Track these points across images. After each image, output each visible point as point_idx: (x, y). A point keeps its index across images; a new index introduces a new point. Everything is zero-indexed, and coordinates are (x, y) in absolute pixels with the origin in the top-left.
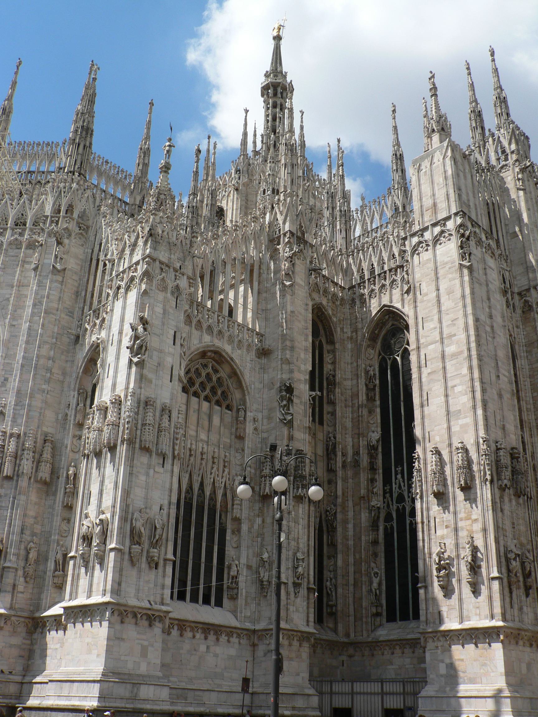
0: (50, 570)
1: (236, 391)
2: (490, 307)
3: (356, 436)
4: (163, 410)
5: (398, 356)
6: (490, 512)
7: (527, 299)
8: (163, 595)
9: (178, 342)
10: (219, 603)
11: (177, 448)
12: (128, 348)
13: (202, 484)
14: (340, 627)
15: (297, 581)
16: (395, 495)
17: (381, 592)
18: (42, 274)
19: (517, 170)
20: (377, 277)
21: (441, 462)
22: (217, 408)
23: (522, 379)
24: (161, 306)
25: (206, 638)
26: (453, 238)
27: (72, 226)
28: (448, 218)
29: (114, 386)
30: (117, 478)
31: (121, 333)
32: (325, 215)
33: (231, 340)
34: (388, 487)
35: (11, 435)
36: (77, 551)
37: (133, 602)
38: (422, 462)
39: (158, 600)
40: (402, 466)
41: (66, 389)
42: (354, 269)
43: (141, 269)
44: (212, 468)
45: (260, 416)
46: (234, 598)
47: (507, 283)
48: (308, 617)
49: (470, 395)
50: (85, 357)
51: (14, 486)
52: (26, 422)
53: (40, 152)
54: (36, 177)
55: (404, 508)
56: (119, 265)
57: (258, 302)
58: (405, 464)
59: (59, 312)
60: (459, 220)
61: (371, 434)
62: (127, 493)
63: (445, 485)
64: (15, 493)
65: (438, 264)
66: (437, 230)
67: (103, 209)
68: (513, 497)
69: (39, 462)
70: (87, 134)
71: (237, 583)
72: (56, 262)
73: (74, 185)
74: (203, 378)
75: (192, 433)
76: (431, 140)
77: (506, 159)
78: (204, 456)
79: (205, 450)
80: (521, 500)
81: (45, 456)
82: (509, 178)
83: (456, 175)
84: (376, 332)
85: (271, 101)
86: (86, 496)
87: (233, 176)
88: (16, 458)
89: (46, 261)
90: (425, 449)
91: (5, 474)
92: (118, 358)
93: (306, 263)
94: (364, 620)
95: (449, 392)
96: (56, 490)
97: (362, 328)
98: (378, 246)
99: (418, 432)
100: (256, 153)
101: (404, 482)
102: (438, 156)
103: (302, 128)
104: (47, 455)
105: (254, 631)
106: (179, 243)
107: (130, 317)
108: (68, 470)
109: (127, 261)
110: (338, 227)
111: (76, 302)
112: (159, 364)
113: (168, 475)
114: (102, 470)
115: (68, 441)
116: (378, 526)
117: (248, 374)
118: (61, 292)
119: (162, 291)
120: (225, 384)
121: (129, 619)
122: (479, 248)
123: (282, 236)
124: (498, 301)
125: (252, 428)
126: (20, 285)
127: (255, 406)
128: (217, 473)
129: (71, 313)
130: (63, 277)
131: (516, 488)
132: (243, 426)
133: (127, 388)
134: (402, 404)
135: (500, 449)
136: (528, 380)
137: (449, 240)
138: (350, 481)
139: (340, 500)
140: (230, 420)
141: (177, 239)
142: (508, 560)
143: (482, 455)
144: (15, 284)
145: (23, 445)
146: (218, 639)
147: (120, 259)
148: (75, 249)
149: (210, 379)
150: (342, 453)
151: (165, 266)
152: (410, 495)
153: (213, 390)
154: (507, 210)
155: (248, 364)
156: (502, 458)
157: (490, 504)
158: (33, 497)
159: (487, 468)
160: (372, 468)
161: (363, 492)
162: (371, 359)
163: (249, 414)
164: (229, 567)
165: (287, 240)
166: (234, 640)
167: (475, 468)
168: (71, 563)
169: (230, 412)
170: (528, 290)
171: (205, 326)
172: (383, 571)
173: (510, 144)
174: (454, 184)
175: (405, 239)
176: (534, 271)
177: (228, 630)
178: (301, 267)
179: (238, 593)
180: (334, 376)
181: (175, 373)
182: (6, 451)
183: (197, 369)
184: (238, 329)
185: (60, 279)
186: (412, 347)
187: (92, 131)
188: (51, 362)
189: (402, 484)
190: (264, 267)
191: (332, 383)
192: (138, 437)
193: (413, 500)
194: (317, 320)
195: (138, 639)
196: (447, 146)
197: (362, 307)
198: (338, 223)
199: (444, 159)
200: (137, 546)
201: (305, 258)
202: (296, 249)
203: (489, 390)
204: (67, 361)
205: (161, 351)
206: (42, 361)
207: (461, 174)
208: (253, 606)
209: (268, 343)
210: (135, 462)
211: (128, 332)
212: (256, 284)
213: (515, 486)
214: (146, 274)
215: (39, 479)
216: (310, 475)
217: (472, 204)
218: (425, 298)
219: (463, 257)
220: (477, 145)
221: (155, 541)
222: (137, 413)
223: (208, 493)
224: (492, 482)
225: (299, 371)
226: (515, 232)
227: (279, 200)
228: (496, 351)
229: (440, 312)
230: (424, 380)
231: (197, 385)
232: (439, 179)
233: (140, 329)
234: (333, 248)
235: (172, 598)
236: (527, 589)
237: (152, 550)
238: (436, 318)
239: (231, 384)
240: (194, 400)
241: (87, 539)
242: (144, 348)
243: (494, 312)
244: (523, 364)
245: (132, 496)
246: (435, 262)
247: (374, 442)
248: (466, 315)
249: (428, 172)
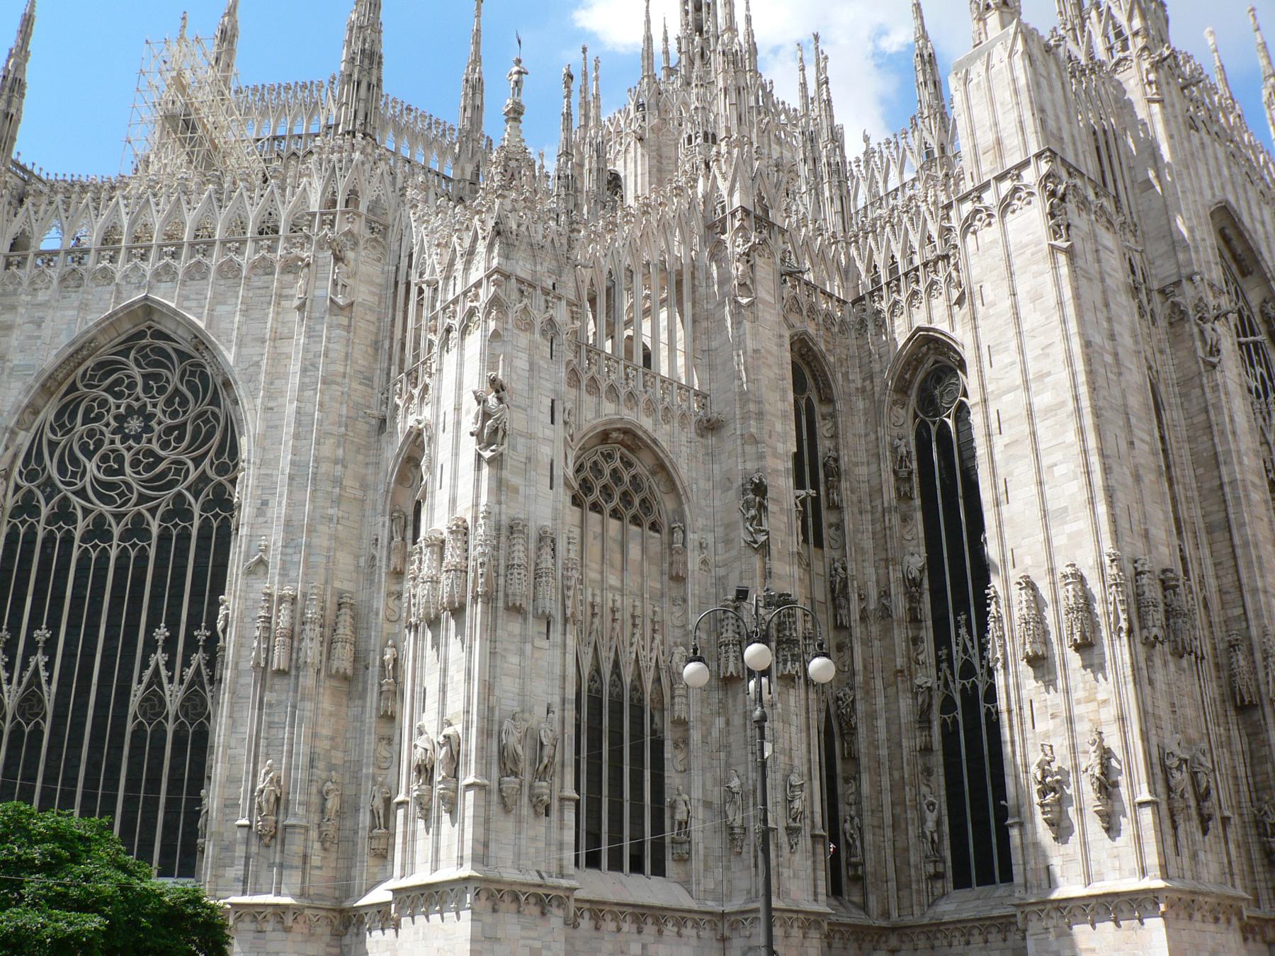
0: (364, 828)
1: (666, 498)
2: (1109, 320)
3: (883, 564)
4: (541, 539)
5: (948, 417)
6: (1131, 686)
7: (1177, 299)
8: (561, 859)
9: (559, 417)
10: (659, 870)
11: (569, 603)
12: (472, 434)
13: (616, 664)
14: (873, 901)
15: (793, 825)
16: (957, 665)
17: (941, 837)
18: (313, 315)
19: (1146, 65)
20: (902, 278)
21: (1037, 603)
22: (634, 529)
23: (1174, 445)
24: (525, 356)
25: (640, 932)
26: (1036, 200)
27: (359, 227)
28: (1025, 164)
29: (453, 502)
30: (470, 661)
31: (458, 409)
32: (801, 173)
33: (650, 408)
34: (945, 651)
35: (281, 599)
36: (408, 792)
37: (510, 874)
38: (1002, 603)
39: (554, 869)
40: (968, 612)
41: (369, 513)
42: (861, 267)
43: (485, 294)
44: (633, 634)
45: (710, 538)
46: (683, 860)
47: (1139, 273)
48: (815, 886)
49: (1083, 480)
50: (398, 455)
51: (292, 685)
52: (305, 574)
53: (292, 101)
54: (289, 145)
55: (975, 686)
56: (445, 290)
57: (694, 338)
58: (972, 609)
59: (347, 380)
60: (1044, 167)
61: (907, 558)
62: (488, 688)
63: (1046, 642)
64: (295, 697)
65: (1012, 248)
66: (1006, 186)
67: (410, 193)
68: (1169, 658)
69: (331, 642)
70: (371, 63)
71: (688, 834)
72: (335, 293)
73: (357, 156)
74: (607, 478)
75: (594, 575)
76: (985, 24)
77: (1125, 48)
78: (618, 616)
79: (618, 604)
80: (1185, 663)
81: (341, 631)
82: (1132, 82)
83: (1036, 84)
84: (907, 376)
86: (417, 696)
87: (632, 115)
88: (292, 638)
89: (318, 293)
90: (1006, 581)
91: (275, 667)
92: (456, 454)
93: (775, 263)
94: (914, 887)
95: (1045, 477)
96: (365, 689)
97: (882, 372)
98: (900, 221)
99: (992, 551)
100: (671, 71)
101: (972, 640)
102: (999, 53)
103: (749, 20)
104: (344, 630)
105: (723, 914)
106: (548, 244)
107: (474, 379)
108: (383, 654)
109: (459, 281)
110: (827, 194)
111: (376, 360)
112: (529, 459)
113: (558, 652)
114: (442, 649)
115: (380, 603)
116: (930, 722)
117: (685, 466)
118: (348, 346)
119: (526, 330)
120: (646, 485)
121: (507, 905)
122: (1084, 214)
123: (729, 217)
124: (1124, 307)
125: (698, 560)
126: (277, 338)
127: (701, 522)
128: (641, 643)
129: (368, 381)
130: (350, 319)
131: (1175, 641)
132: (681, 558)
133: (476, 505)
134: (961, 501)
135: (1142, 573)
136: (1186, 446)
137: (1029, 203)
138: (877, 643)
139: (859, 679)
140: (658, 549)
141: (544, 237)
142: (1166, 770)
143: (1111, 586)
144: (268, 336)
145: (303, 614)
146: (660, 932)
147: (447, 278)
148: (367, 268)
149: (618, 478)
150: (860, 595)
151: (526, 286)
152: (984, 662)
153: (626, 499)
154: (1130, 141)
155: (684, 449)
156: (1146, 589)
157: (1129, 671)
158: (327, 704)
159: (1120, 608)
160: (915, 620)
161: (900, 662)
162: (901, 425)
163: (690, 536)
164: (673, 806)
165: (737, 224)
166: (689, 931)
167: (1099, 609)
168: (400, 812)
169: (657, 535)
170: (1178, 284)
171: (603, 386)
172: (944, 799)
173: (1130, 19)
174: (1031, 102)
175: (948, 207)
176: (1186, 248)
177: (678, 914)
178: (766, 271)
179: (690, 849)
180: (836, 460)
181: (558, 472)
182: (273, 626)
183: (595, 463)
184: (662, 388)
185: (345, 321)
186: (973, 400)
187: (380, 57)
188: (339, 467)
189: (969, 645)
190: (700, 275)
191: (834, 473)
192: (501, 588)
193: (991, 672)
194: (800, 362)
195: (523, 938)
196: (1016, 33)
197: (879, 334)
198: (826, 187)
199: (1010, 56)
200: (512, 778)
201: (772, 254)
202: (754, 238)
203: (1115, 466)
204: (367, 464)
205: (530, 436)
206: (324, 468)
207: (1044, 83)
208: (718, 872)
209: (716, 410)
210: (499, 632)
211: (471, 408)
212: (688, 306)
213: (1172, 638)
214: (495, 302)
215: (334, 671)
216: (805, 638)
217: (1066, 136)
218: (991, 311)
219: (1055, 233)
220: (1069, 26)
221: (542, 767)
222: (497, 548)
223: (627, 679)
224: (1130, 632)
225: (775, 455)
226: (1149, 180)
227: (718, 153)
228: (1124, 397)
229: (1020, 333)
230: (997, 457)
231: (597, 492)
232: (1003, 94)
233: (492, 400)
234: (819, 231)
235: (577, 864)
236: (1205, 820)
237: (537, 783)
238: (1013, 345)
239: (656, 485)
240: (594, 517)
241: (425, 771)
242: (500, 433)
243: (1117, 328)
244: (1175, 417)
245: (497, 692)
246: (1006, 246)
247: (915, 573)
248: (1067, 338)
249: (984, 85)
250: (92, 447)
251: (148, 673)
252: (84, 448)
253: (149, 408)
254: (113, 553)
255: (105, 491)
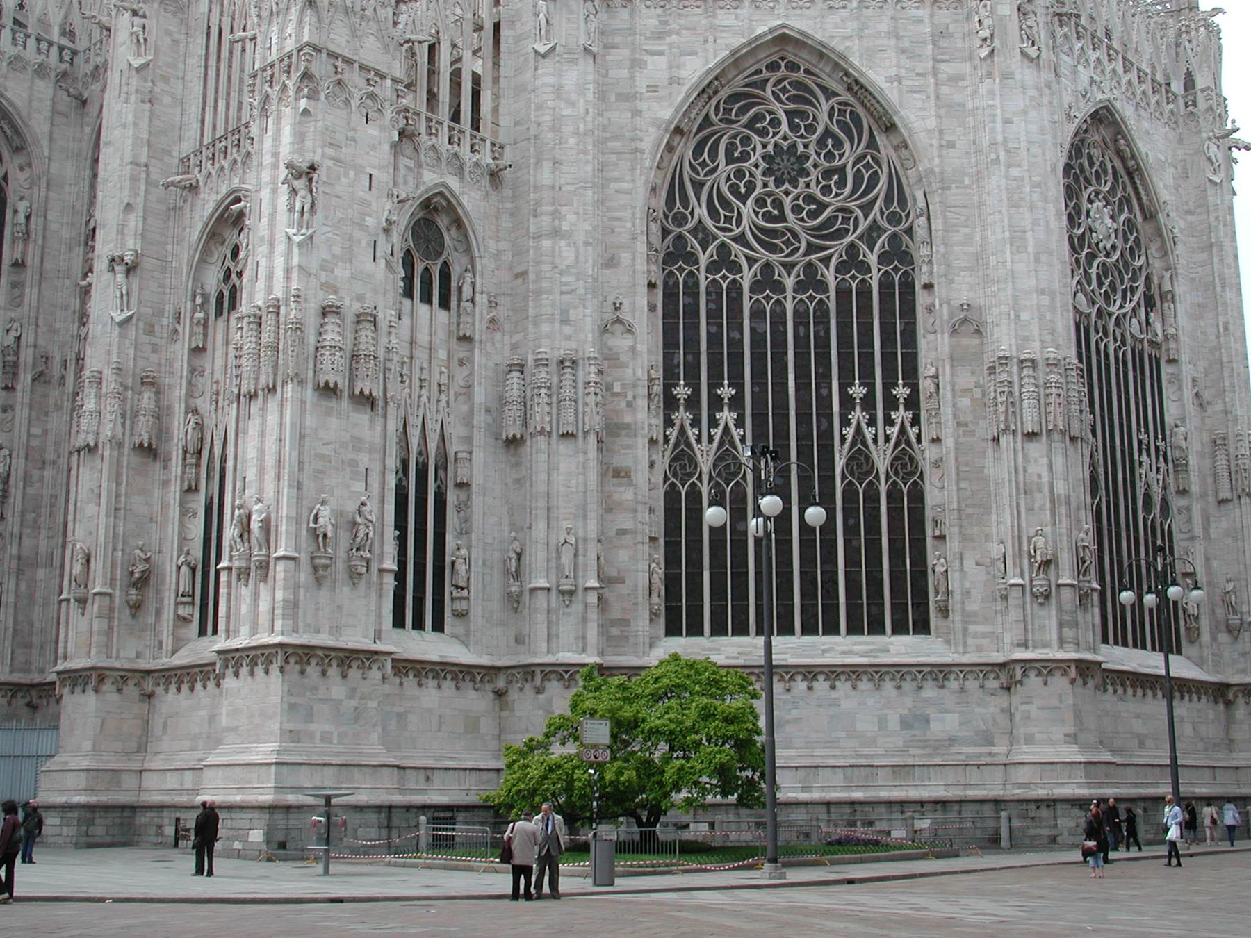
250: (743, 190)
251: (850, 432)
252: (734, 190)
253: (801, 149)
254: (789, 307)
255: (768, 238)
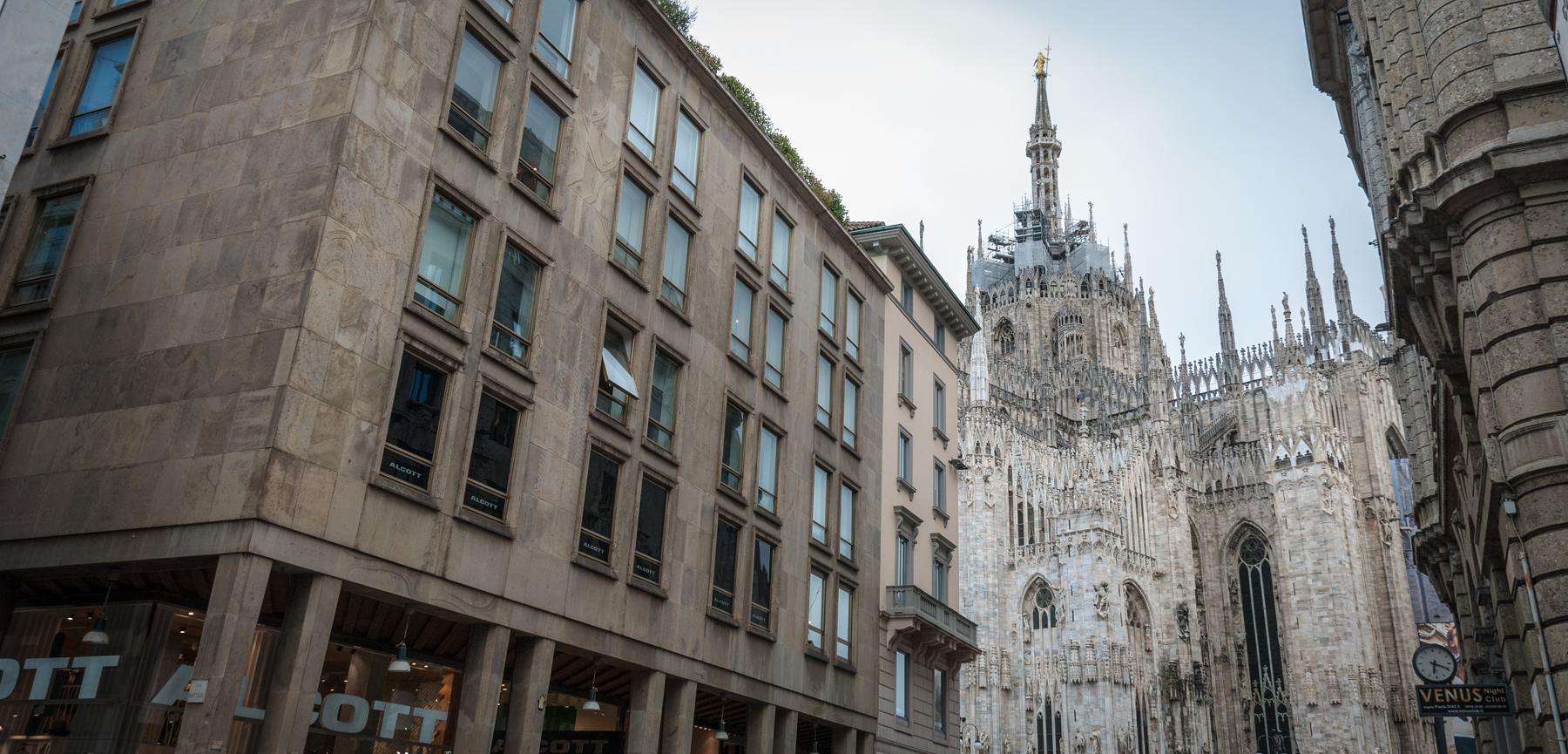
43: (1093, 538)
85: (1042, 168)
161: (1235, 685)
162: (1232, 567)
209: (1160, 567)
214: (1099, 543)
